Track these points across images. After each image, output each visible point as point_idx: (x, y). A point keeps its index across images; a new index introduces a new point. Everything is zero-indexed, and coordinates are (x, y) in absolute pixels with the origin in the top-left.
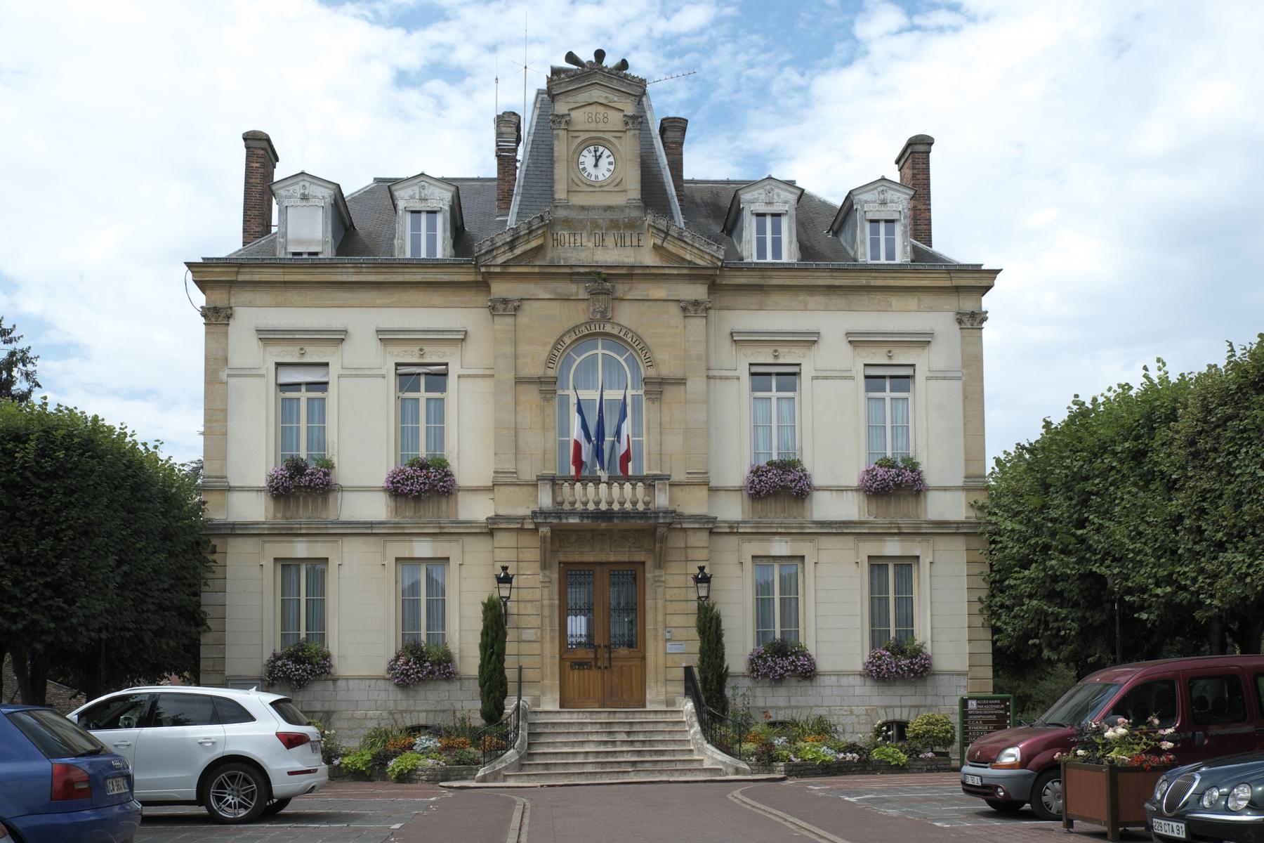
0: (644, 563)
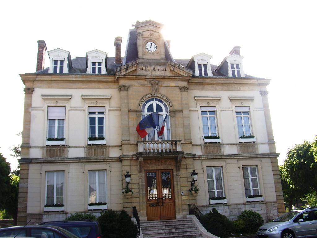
0: (172, 169)
